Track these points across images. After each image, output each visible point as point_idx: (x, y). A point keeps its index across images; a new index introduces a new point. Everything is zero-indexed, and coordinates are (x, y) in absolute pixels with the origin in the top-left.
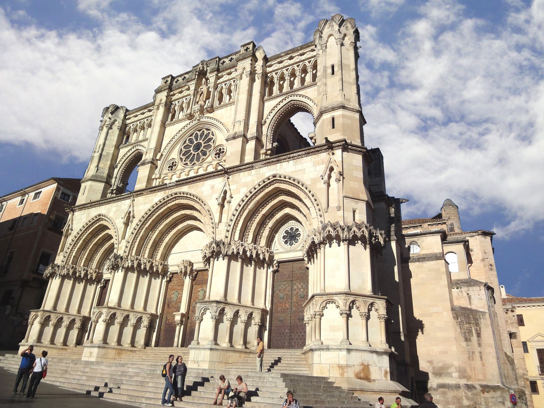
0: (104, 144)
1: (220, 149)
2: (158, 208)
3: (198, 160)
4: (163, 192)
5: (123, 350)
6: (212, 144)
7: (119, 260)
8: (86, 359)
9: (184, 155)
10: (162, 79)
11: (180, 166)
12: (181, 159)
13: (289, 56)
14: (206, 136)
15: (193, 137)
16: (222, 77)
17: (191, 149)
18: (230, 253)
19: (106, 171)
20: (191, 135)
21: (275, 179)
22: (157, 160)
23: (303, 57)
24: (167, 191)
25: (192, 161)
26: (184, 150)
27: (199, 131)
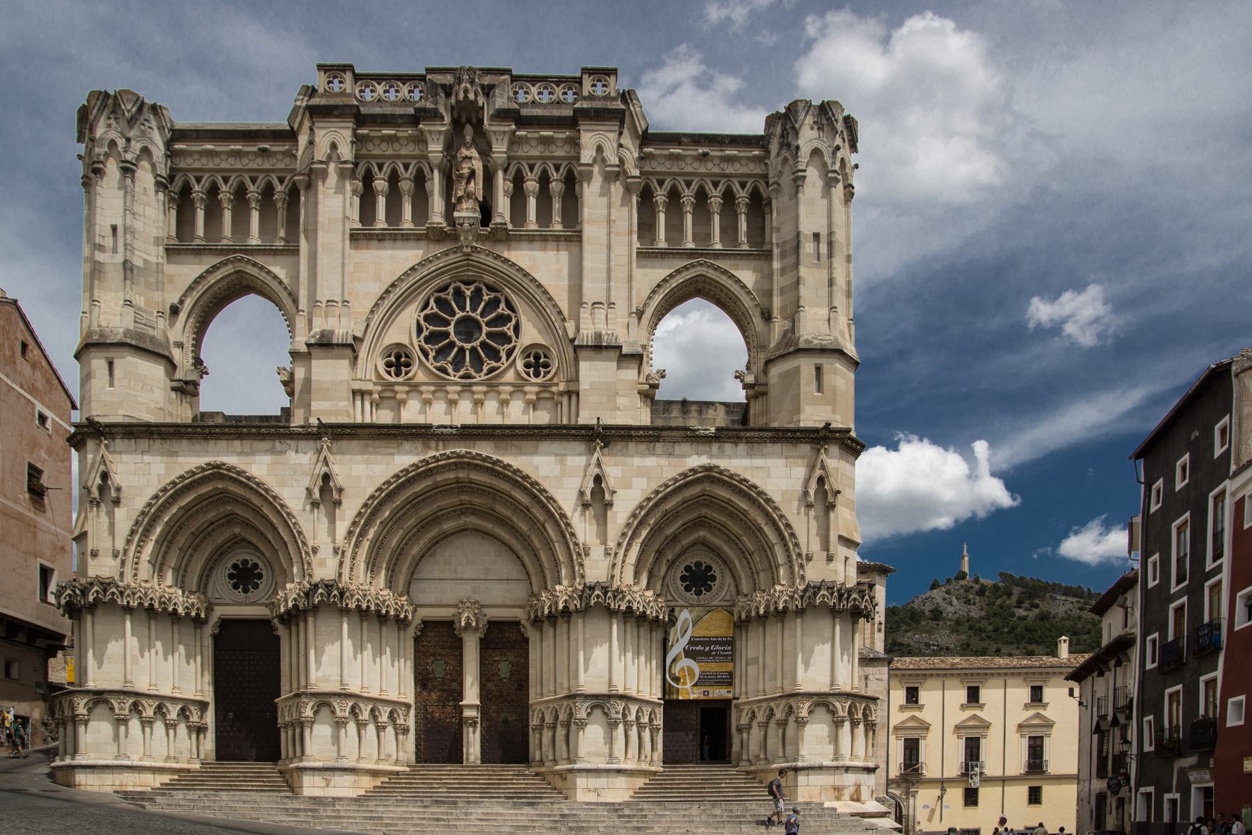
1: (537, 357)
2: (410, 482)
6: (511, 333)
8: (317, 793)
9: (428, 340)
12: (426, 355)
14: (487, 304)
17: (451, 329)
18: (623, 607)
21: (710, 475)
22: (355, 338)
26: (429, 329)
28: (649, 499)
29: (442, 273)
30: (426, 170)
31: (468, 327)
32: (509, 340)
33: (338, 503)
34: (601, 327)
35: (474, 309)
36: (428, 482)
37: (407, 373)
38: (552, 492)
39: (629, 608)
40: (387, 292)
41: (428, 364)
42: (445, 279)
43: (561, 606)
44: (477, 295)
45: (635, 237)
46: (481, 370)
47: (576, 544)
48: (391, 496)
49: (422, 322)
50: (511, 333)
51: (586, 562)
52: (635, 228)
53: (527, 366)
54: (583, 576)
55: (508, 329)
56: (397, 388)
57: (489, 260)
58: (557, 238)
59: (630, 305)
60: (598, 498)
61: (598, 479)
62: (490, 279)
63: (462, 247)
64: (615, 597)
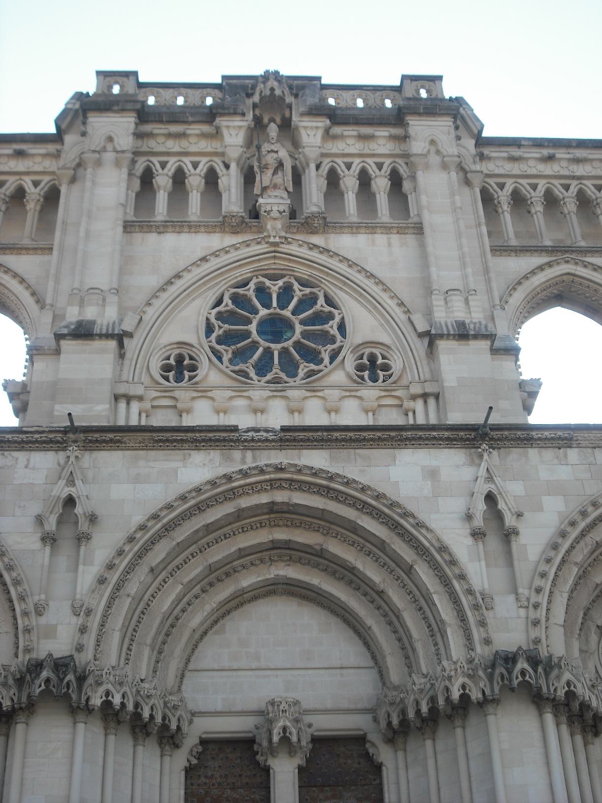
1: (372, 358)
2: (200, 508)
4: (215, 455)
6: (334, 331)
7: (70, 677)
9: (219, 341)
10: (99, 73)
13: (546, 152)
14: (300, 302)
15: (250, 291)
16: (341, 137)
17: (253, 327)
18: (561, 693)
20: (245, 284)
23: (579, 170)
24: (237, 454)
27: (274, 278)
28: (573, 524)
29: (240, 266)
30: (220, 169)
31: (275, 328)
32: (333, 341)
33: (82, 538)
34: (460, 314)
35: (283, 306)
36: (228, 508)
37: (191, 378)
38: (422, 517)
39: (571, 695)
40: (170, 283)
41: (223, 367)
42: (244, 273)
43: (456, 695)
44: (287, 291)
45: (484, 229)
46: (295, 375)
47: (470, 592)
48: (168, 528)
49: (213, 320)
50: (334, 331)
51: (490, 621)
52: (483, 220)
53: (360, 368)
54: (487, 642)
55: (332, 328)
56: (176, 394)
57: (304, 252)
58: (387, 229)
59: (491, 298)
60: (495, 524)
61: (490, 498)
62: (304, 272)
63: (269, 236)
64: (547, 674)
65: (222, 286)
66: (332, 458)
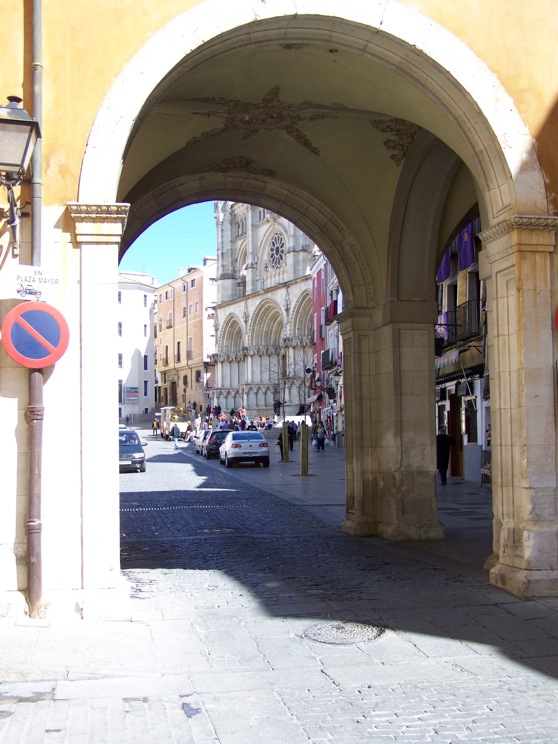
0: (222, 243)
2: (260, 309)
3: (279, 264)
5: (260, 410)
7: (245, 351)
11: (270, 269)
15: (274, 240)
19: (230, 268)
25: (276, 264)
27: (277, 234)
48: (257, 315)
55: (284, 248)
65: (269, 241)
66: (272, 295)
